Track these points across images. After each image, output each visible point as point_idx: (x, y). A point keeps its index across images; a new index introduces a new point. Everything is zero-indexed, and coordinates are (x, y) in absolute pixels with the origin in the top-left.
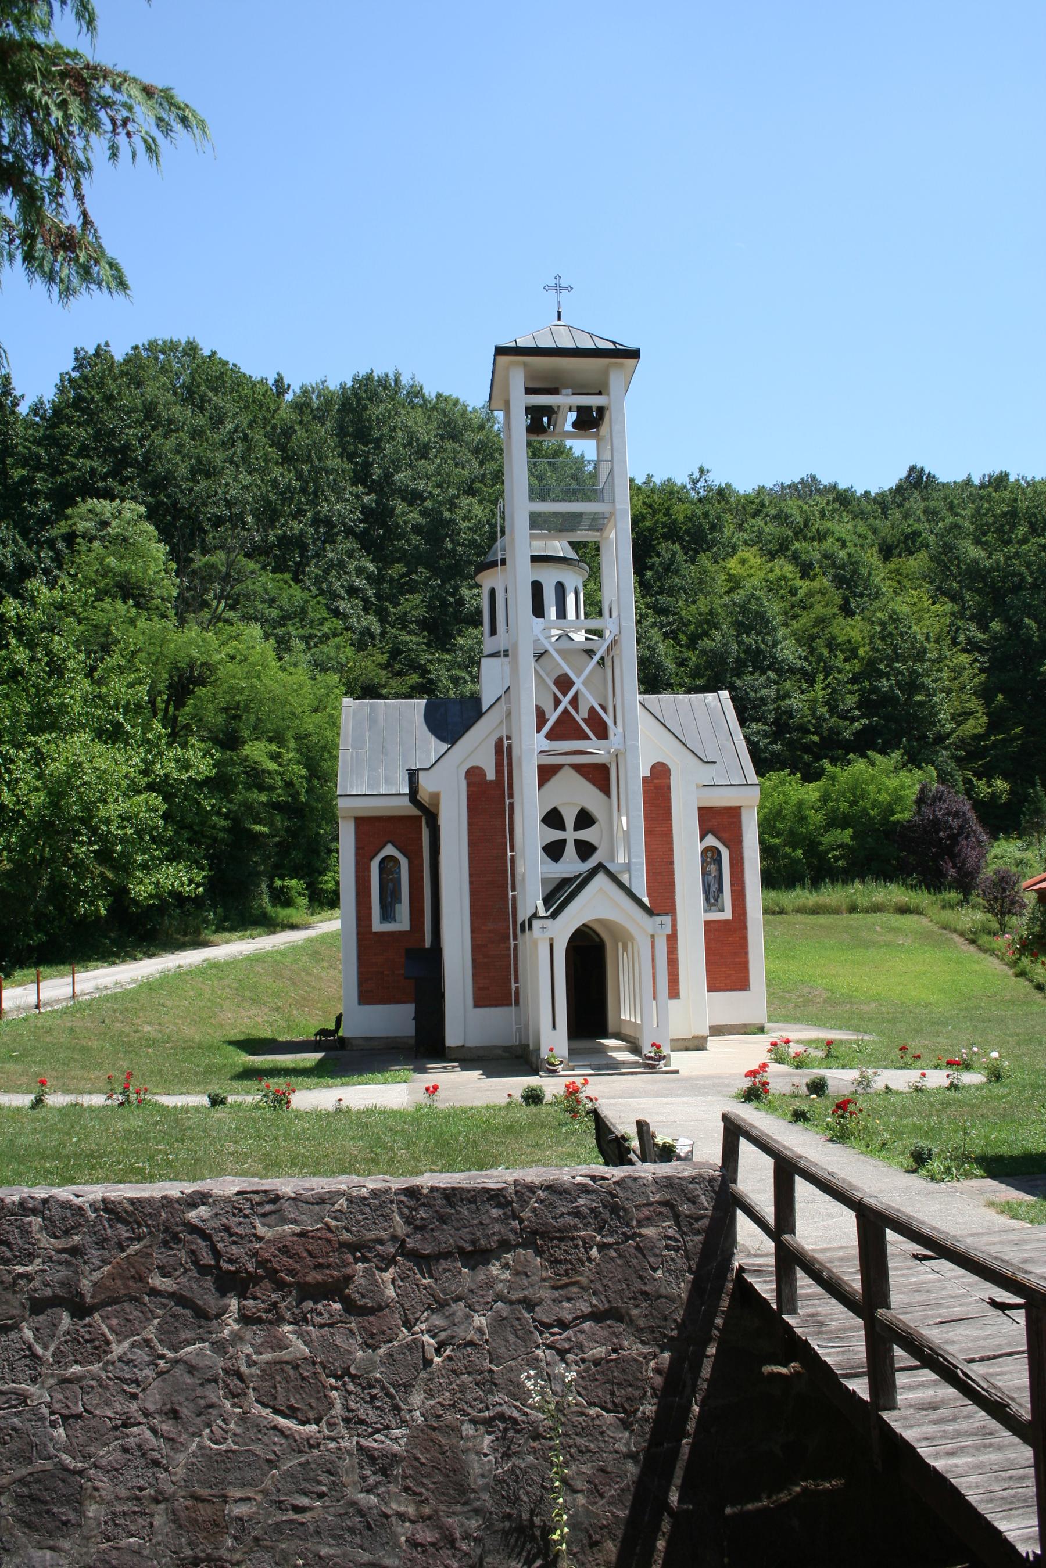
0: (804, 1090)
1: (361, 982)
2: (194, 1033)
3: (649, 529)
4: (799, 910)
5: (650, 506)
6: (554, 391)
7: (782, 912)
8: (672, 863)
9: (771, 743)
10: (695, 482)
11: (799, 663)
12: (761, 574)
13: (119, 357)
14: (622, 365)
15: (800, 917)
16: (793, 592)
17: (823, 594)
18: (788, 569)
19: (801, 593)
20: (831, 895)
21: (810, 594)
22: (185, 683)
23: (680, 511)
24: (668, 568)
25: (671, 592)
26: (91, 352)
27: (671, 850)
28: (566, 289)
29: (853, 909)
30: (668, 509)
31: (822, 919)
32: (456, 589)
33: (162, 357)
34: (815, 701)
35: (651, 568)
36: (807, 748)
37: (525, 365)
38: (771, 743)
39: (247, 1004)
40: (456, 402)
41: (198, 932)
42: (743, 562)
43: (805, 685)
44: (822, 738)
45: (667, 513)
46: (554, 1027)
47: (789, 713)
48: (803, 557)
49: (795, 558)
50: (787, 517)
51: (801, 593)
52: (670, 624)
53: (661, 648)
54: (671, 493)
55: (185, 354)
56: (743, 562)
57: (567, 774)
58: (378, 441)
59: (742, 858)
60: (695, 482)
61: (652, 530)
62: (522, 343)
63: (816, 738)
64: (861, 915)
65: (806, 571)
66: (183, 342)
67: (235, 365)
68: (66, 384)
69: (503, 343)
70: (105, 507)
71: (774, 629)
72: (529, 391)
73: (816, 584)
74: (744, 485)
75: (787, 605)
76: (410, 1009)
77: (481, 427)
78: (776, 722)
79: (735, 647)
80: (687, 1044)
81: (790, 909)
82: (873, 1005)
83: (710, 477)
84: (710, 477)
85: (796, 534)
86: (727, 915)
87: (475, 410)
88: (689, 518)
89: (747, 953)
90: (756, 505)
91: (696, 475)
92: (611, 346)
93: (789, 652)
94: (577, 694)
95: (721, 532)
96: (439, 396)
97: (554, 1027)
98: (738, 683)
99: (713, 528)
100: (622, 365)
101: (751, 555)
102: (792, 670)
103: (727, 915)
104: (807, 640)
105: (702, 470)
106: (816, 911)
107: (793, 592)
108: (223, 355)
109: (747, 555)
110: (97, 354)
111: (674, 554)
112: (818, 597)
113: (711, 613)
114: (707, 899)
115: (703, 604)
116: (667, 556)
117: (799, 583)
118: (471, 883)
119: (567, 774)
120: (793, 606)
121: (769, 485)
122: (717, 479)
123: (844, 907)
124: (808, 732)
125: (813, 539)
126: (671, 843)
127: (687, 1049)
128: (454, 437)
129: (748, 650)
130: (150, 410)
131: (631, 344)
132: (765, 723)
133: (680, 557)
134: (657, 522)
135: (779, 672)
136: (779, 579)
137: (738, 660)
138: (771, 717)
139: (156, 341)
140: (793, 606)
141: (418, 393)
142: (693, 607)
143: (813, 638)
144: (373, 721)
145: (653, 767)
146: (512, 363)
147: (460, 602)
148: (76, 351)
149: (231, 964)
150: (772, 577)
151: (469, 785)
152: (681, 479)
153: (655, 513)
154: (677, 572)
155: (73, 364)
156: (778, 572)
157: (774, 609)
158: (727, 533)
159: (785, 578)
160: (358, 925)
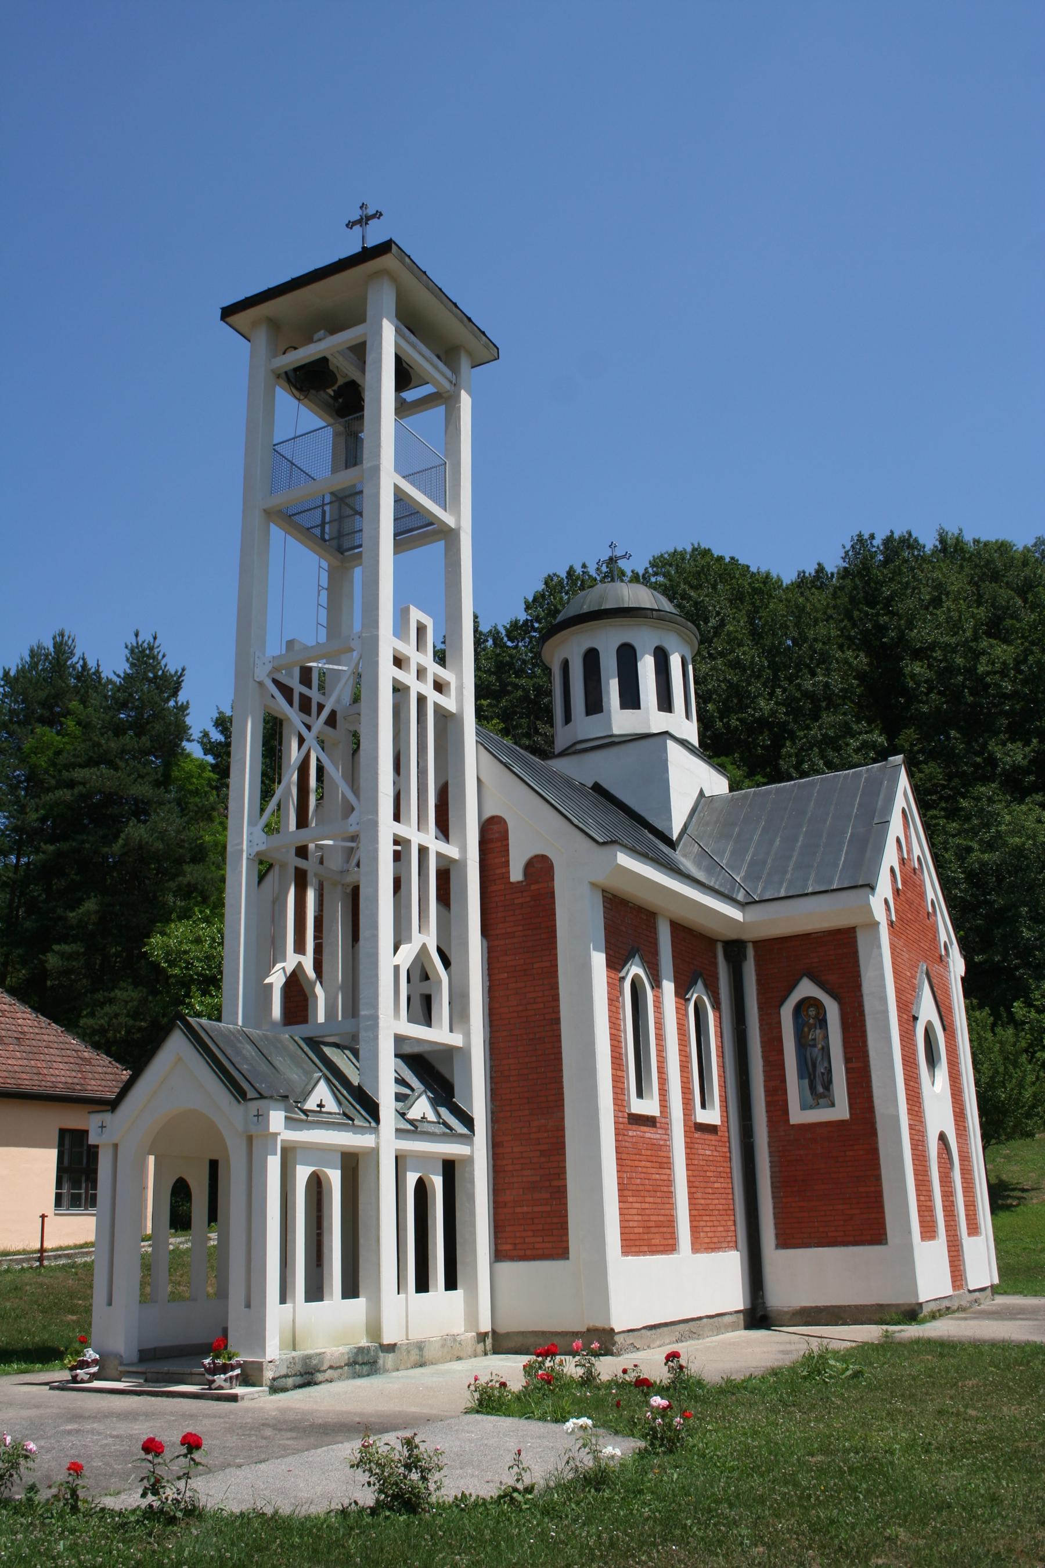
8: (557, 1021)
27: (556, 998)
28: (373, 216)
32: (984, 746)
46: (110, 1304)
58: (889, 600)
59: (862, 1013)
66: (689, 549)
67: (732, 558)
86: (840, 1110)
89: (878, 1178)
96: (977, 542)
97: (110, 1304)
103: (840, 1110)
114: (812, 1087)
126: (555, 987)
128: (996, 577)
139: (662, 555)
147: (992, 761)
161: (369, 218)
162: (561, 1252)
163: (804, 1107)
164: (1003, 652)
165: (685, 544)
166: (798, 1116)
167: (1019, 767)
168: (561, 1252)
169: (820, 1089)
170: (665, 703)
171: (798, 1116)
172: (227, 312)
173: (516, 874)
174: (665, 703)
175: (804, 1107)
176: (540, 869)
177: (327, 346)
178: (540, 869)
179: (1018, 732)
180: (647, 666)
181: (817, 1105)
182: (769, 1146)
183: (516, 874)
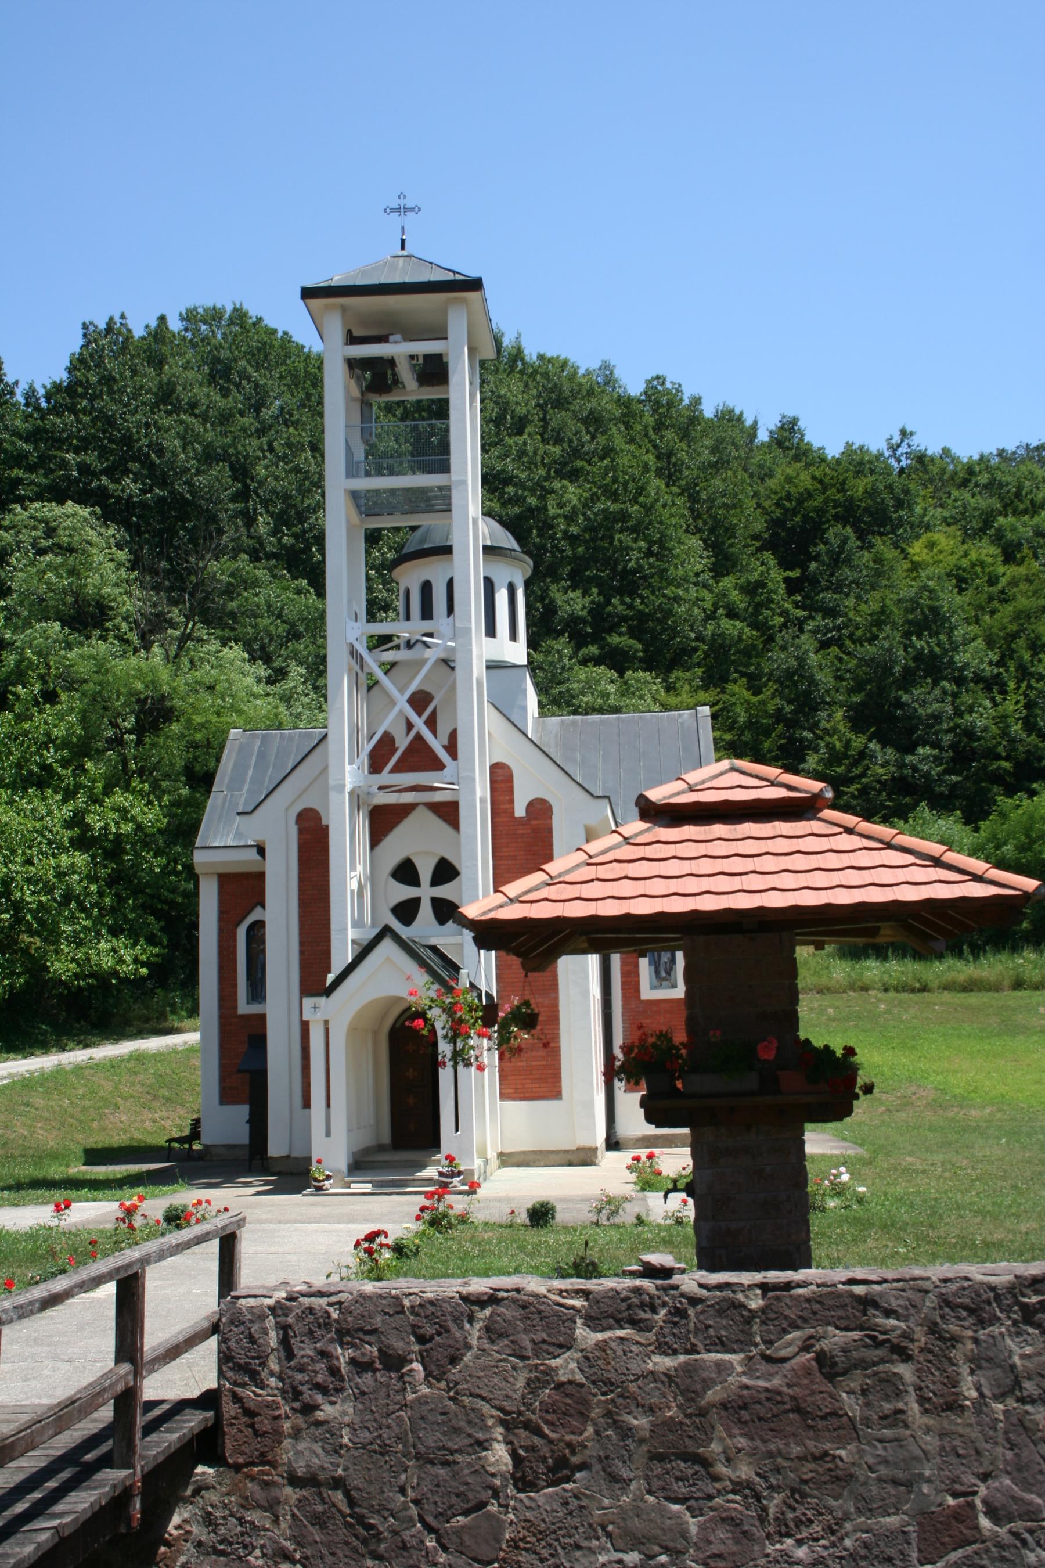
0: (523, 1218)
1: (223, 1078)
2: (48, 1138)
3: (816, 510)
4: (947, 987)
5: (821, 482)
6: (382, 339)
7: (924, 989)
9: (946, 772)
10: (894, 448)
11: (989, 671)
12: (952, 560)
13: (138, 332)
14: (464, 301)
15: (946, 996)
16: (992, 581)
17: (1031, 582)
18: (986, 551)
19: (1003, 581)
20: (993, 966)
21: (1014, 582)
22: (155, 713)
23: (859, 486)
24: (837, 559)
25: (838, 588)
26: (102, 326)
28: (412, 210)
29: (1018, 985)
30: (844, 483)
31: (973, 999)
33: (203, 327)
34: (1004, 717)
35: (816, 558)
36: (997, 778)
37: (344, 309)
38: (946, 772)
39: (156, 1104)
40: (565, 364)
41: (162, 1016)
42: (931, 545)
43: (999, 698)
44: (1018, 764)
45: (842, 490)
46: (328, 1134)
47: (969, 733)
48: (1009, 535)
49: (998, 538)
50: (1001, 485)
51: (1003, 581)
52: (839, 629)
53: (813, 659)
54: (861, 463)
55: (231, 322)
56: (931, 545)
57: (422, 813)
60: (894, 448)
61: (821, 511)
62: (337, 280)
63: (1006, 765)
64: (1026, 993)
65: (1010, 554)
67: (285, 333)
68: (78, 363)
69: (310, 283)
70: (52, 510)
71: (952, 629)
72: (352, 339)
73: (1022, 570)
74: (967, 450)
75: (983, 597)
76: (243, 1111)
77: (591, 392)
78: (953, 746)
79: (901, 653)
80: (574, 1158)
81: (934, 984)
82: (988, 1111)
83: (915, 441)
84: (915, 441)
85: (1005, 507)
87: (588, 373)
88: (871, 493)
90: (968, 475)
91: (897, 439)
92: (450, 277)
93: (974, 655)
94: (434, 713)
95: (910, 509)
96: (541, 357)
97: (328, 1134)
98: (905, 698)
99: (899, 504)
100: (464, 301)
101: (945, 539)
102: (978, 679)
104: (1004, 644)
105: (904, 433)
106: (968, 987)
107: (992, 581)
108: (270, 322)
109: (936, 536)
110: (109, 328)
111: (845, 541)
112: (1024, 586)
113: (883, 611)
114: (657, 972)
115: (873, 602)
116: (835, 542)
117: (1001, 569)
118: (302, 952)
119: (422, 813)
120: (991, 599)
121: (1010, 447)
122: (930, 443)
123: (1006, 983)
124: (998, 757)
125: (1025, 512)
127: (570, 1164)
129: (919, 657)
130: (166, 395)
131: (472, 273)
132: (933, 746)
133: (853, 543)
134: (826, 501)
135: (960, 681)
136: (973, 565)
137: (907, 671)
138: (947, 739)
139: (195, 309)
140: (991, 599)
141: (518, 354)
142: (863, 607)
143: (1014, 636)
144: (262, 756)
145: (531, 806)
146: (327, 307)
148: (85, 326)
149: (158, 1057)
150: (965, 563)
151: (301, 831)
152: (876, 444)
153: (825, 489)
154: (848, 561)
155: (81, 342)
156: (973, 556)
157: (950, 600)
158: (918, 510)
159: (982, 564)
160: (221, 1006)
161: (407, 210)
162: (555, 1094)
163: (653, 987)
164: (573, 493)
165: (224, 298)
166: (648, 992)
167: (579, 618)
168: (555, 1094)
169: (663, 974)
170: (513, 637)
171: (648, 992)
172: (308, 293)
173: (520, 811)
174: (513, 637)
175: (653, 987)
176: (540, 809)
177: (397, 349)
178: (540, 809)
179: (577, 581)
180: (502, 598)
181: (660, 986)
182: (623, 1015)
183: (520, 811)
